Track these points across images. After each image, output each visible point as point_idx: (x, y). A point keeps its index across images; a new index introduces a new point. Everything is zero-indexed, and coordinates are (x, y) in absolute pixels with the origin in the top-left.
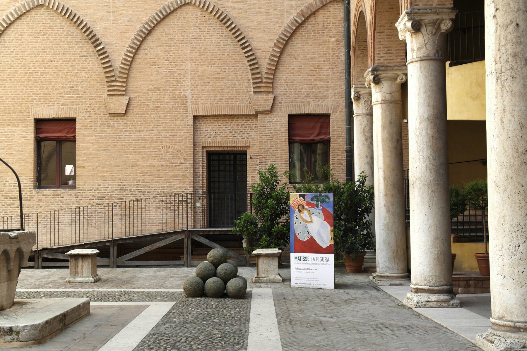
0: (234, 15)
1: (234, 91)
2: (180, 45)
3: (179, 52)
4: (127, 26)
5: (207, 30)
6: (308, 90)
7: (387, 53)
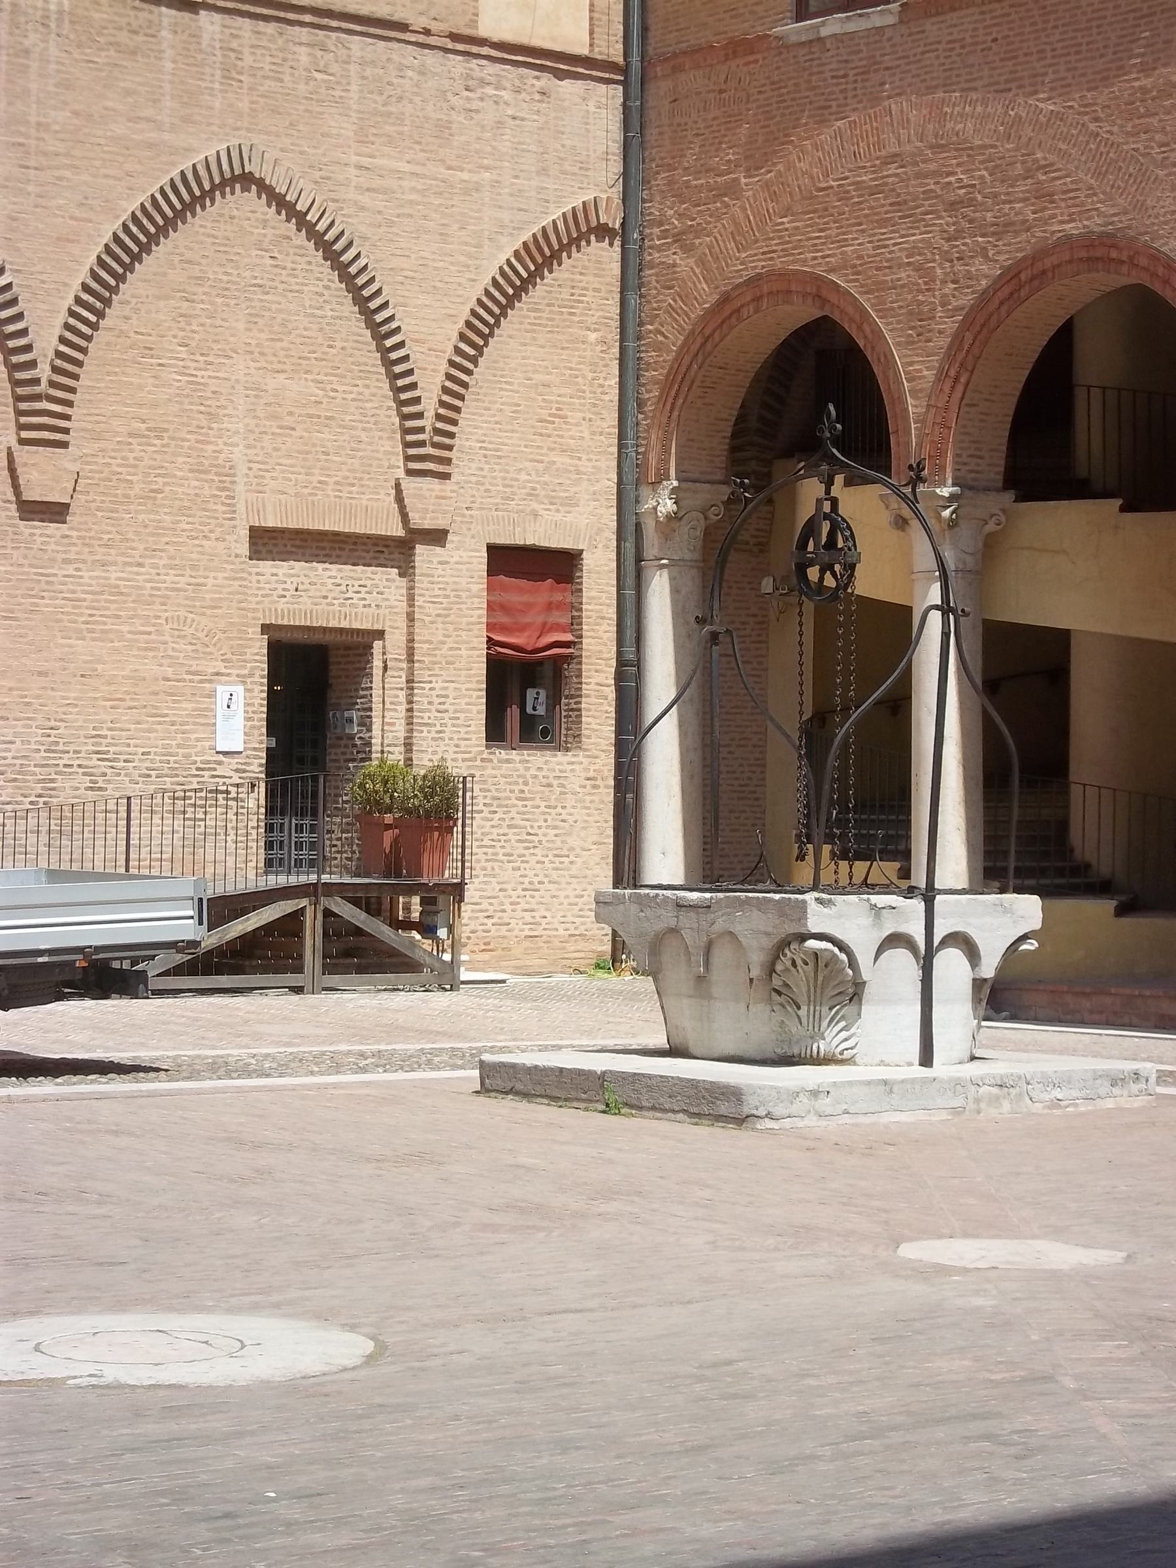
0: (363, 228)
2: (219, 300)
3: (219, 322)
4: (76, 219)
6: (534, 477)
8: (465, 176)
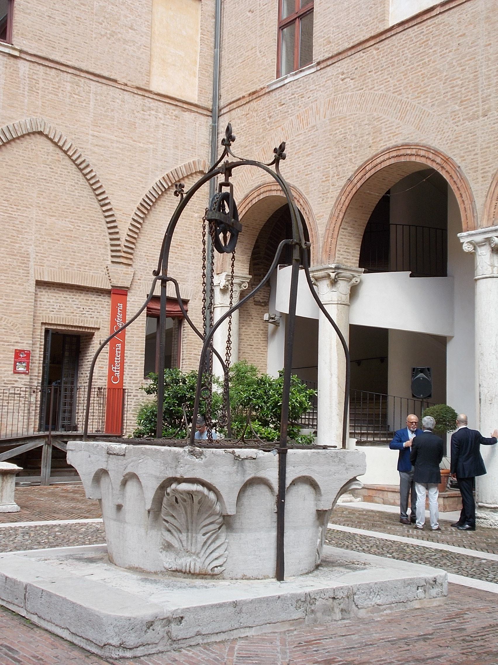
1: (88, 257)
2: (25, 184)
3: (24, 193)
5: (59, 172)
7: (345, 252)
8: (141, 145)
